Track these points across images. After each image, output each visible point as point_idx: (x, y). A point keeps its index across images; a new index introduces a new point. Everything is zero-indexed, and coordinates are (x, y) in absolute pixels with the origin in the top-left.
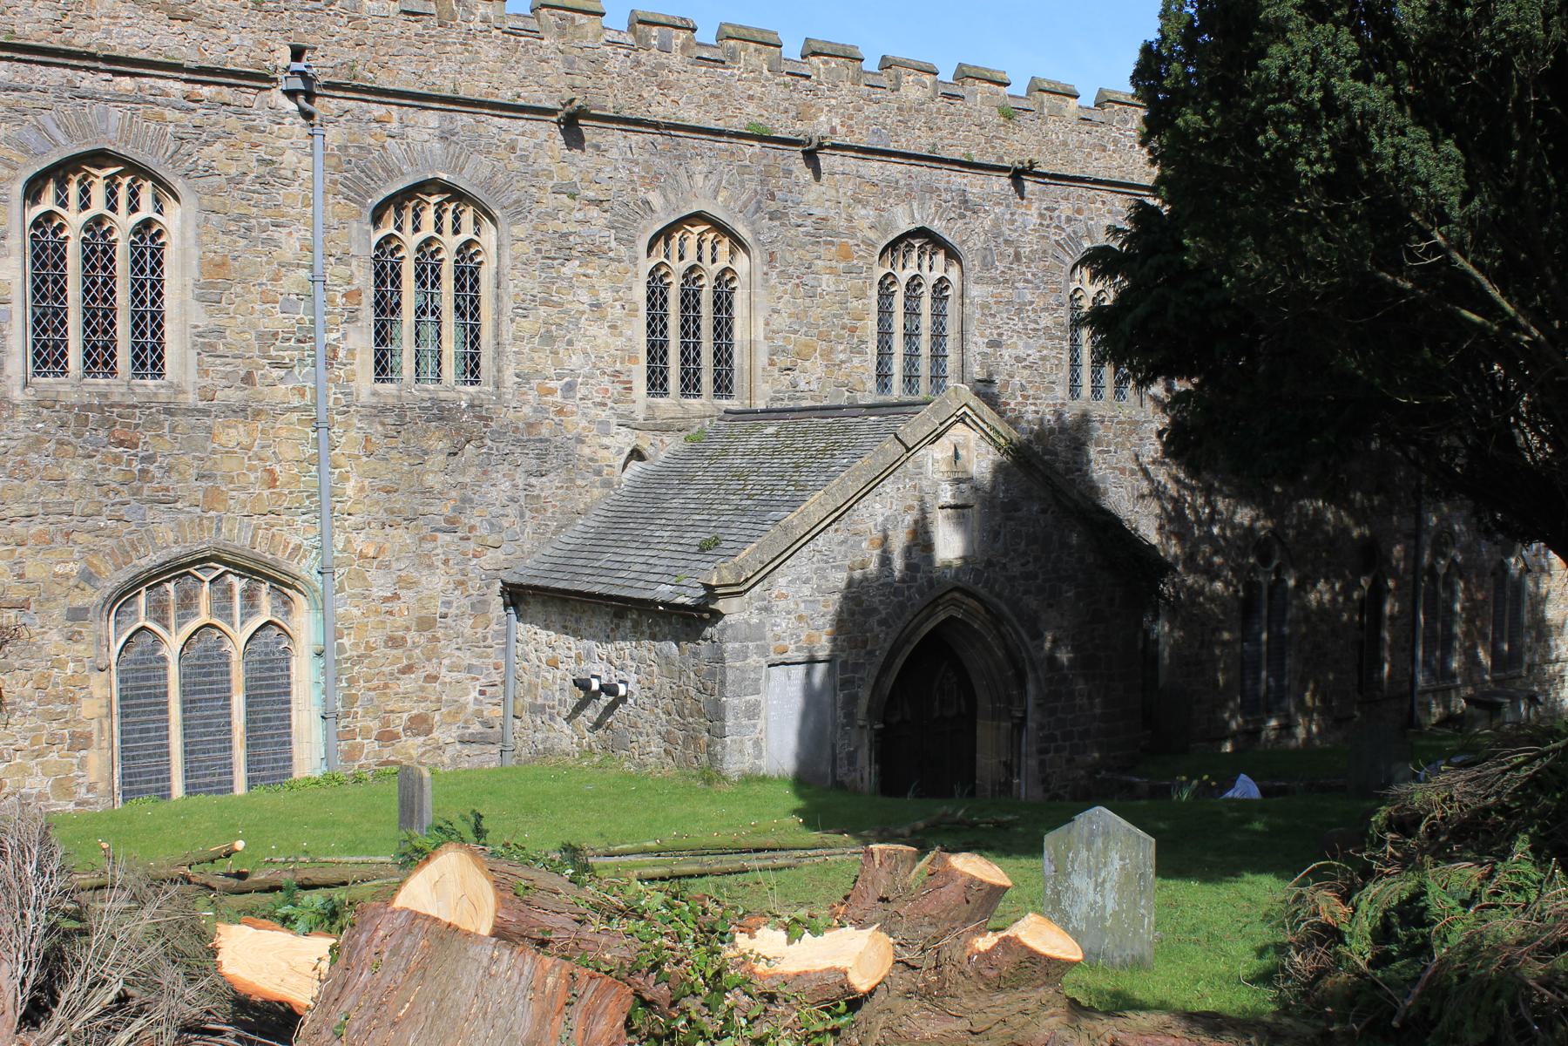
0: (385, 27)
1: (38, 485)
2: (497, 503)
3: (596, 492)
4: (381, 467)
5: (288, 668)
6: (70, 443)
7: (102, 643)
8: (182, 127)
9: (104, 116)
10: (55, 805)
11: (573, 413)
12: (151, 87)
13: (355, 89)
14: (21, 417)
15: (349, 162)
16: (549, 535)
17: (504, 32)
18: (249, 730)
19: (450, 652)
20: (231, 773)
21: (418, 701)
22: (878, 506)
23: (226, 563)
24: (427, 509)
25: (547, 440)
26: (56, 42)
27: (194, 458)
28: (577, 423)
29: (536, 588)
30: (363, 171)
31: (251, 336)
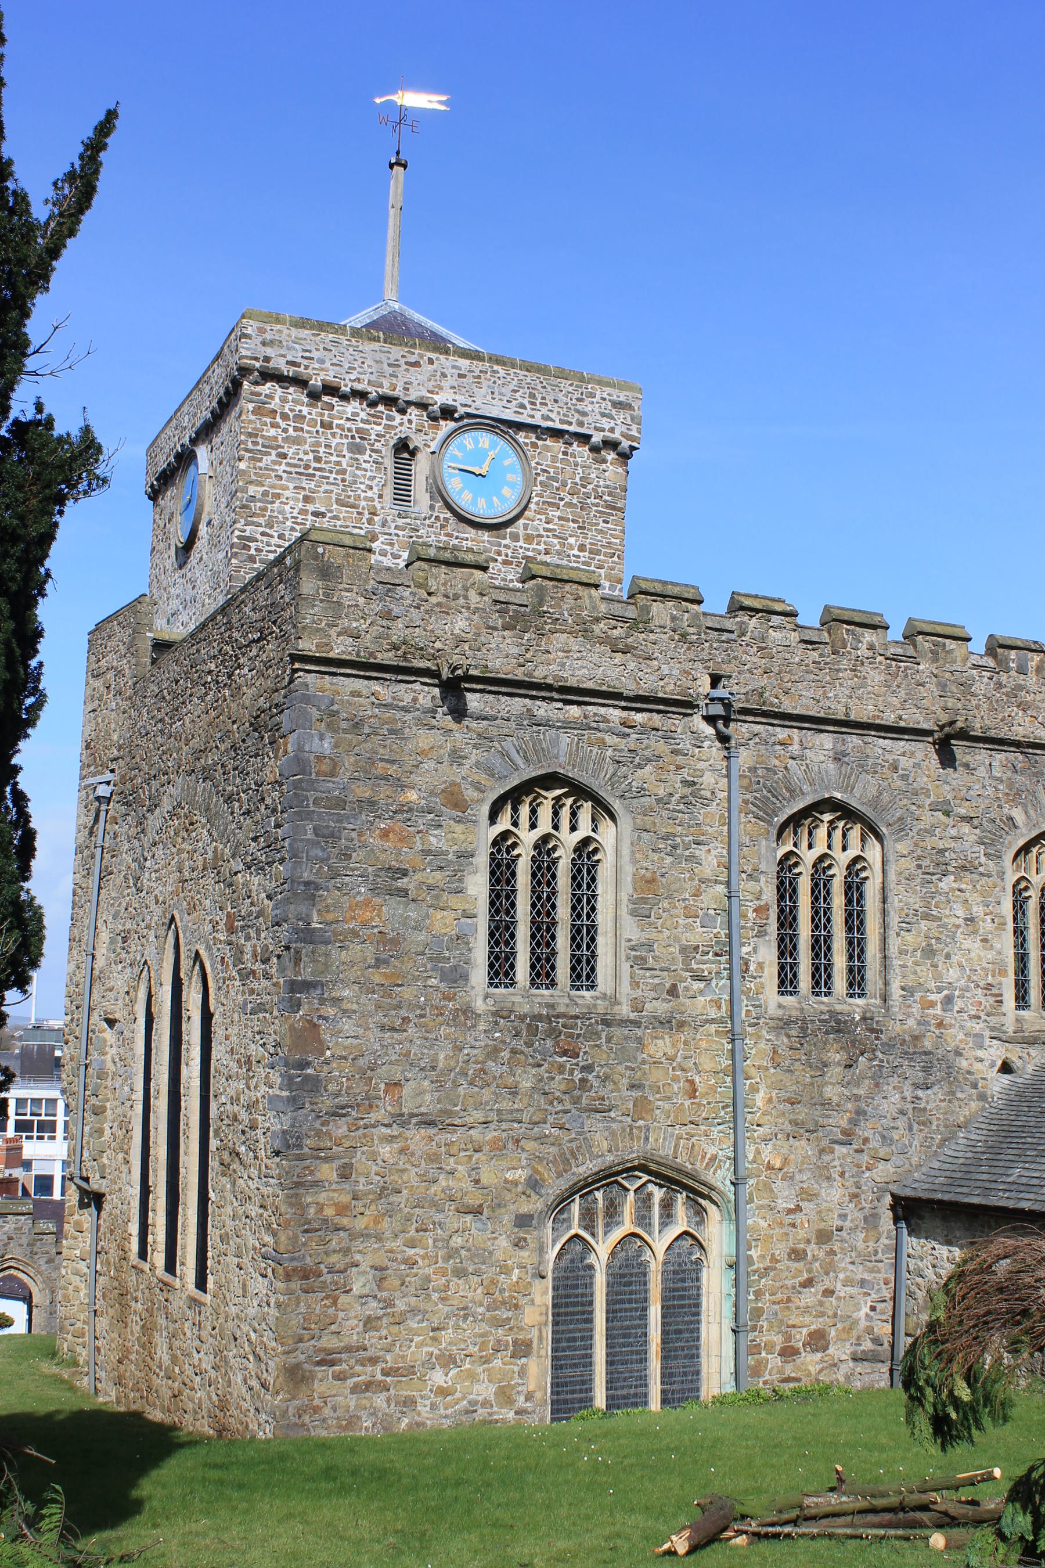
0: (788, 656)
1: (494, 1093)
2: (888, 1115)
3: (974, 1105)
4: (786, 1078)
5: (698, 1279)
6: (522, 1052)
7: (541, 1250)
8: (620, 751)
9: (555, 742)
10: (498, 1413)
11: (951, 1026)
12: (595, 714)
13: (764, 714)
14: (482, 1026)
15: (758, 783)
16: (934, 1148)
17: (887, 659)
18: (663, 1342)
19: (846, 1267)
20: (646, 1385)
21: (816, 1316)
23: (649, 1172)
24: (826, 1121)
25: (930, 1053)
26: (519, 675)
27: (627, 1068)
28: (955, 1036)
29: (940, 1202)
30: (770, 791)
31: (675, 949)
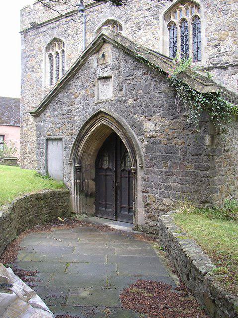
22: (77, 82)
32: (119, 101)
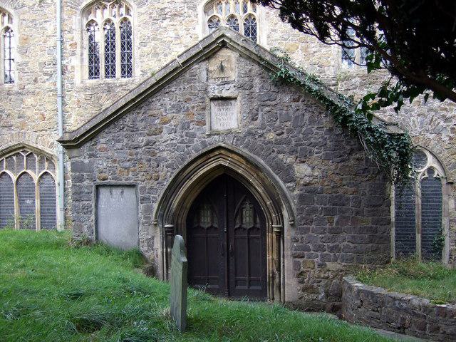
22: (167, 99)
32: (249, 133)
